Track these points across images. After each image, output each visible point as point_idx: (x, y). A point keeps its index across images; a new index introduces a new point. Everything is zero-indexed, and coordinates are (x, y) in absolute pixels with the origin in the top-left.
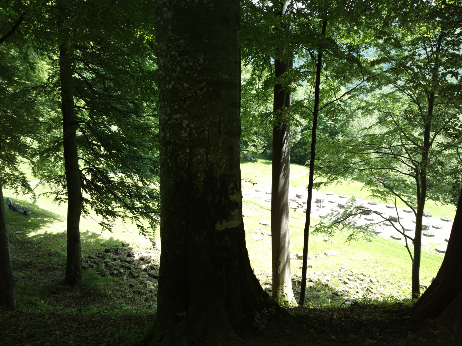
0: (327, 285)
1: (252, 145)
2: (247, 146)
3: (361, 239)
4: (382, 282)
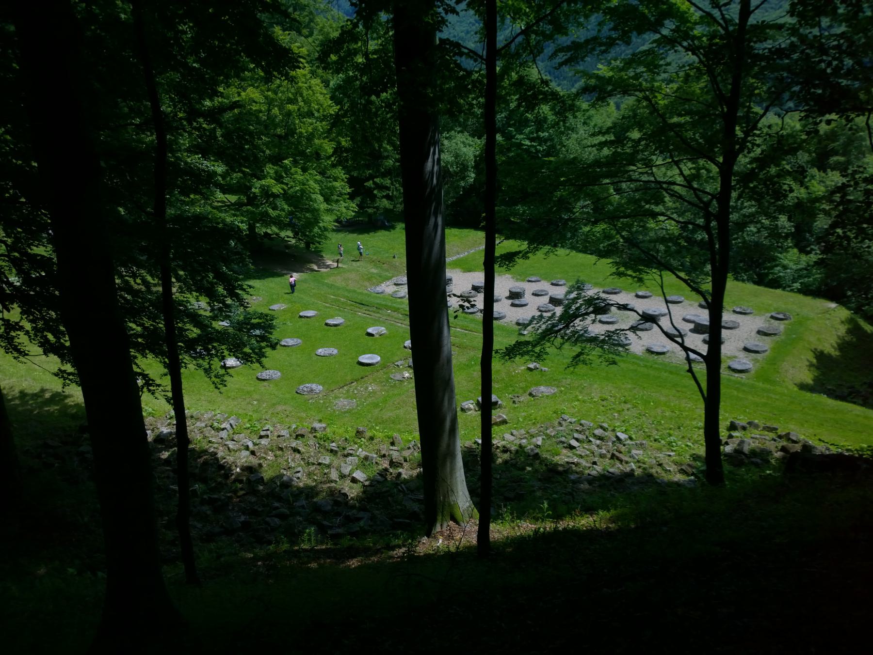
0: (537, 454)
1: (384, 197)
2: (373, 198)
4: (639, 439)
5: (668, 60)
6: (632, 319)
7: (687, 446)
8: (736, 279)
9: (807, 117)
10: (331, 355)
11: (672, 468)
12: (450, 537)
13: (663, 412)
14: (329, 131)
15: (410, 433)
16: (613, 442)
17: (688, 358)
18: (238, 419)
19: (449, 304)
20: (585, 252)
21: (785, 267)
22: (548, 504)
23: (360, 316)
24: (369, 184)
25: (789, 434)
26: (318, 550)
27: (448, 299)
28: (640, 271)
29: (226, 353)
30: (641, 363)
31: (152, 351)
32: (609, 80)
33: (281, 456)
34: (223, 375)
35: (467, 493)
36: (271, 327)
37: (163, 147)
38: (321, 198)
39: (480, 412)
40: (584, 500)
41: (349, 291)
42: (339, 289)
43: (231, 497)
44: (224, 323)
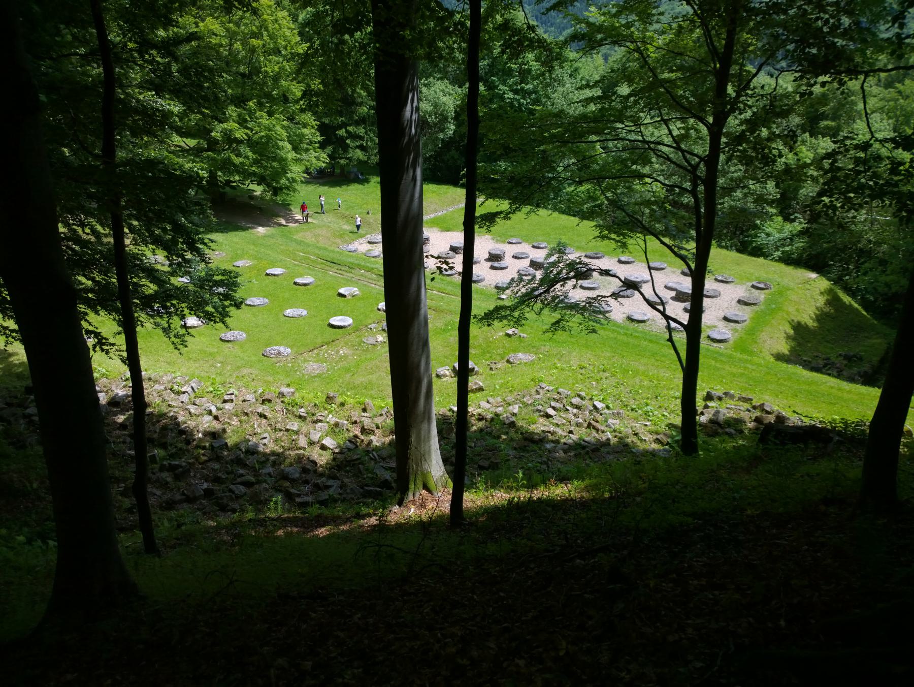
0: (513, 423)
1: (357, 147)
2: (346, 148)
3: (576, 329)
4: (616, 407)
5: (661, 9)
6: (614, 285)
7: (664, 415)
8: (720, 246)
9: (801, 77)
10: (300, 316)
11: (648, 437)
12: (423, 505)
13: (641, 381)
14: (298, 72)
15: (383, 399)
16: (591, 411)
17: (668, 327)
18: (200, 382)
19: (426, 265)
20: (570, 215)
21: (768, 235)
22: (523, 474)
23: (331, 276)
24: (342, 132)
25: (763, 404)
26: (284, 520)
27: (425, 260)
28: (624, 235)
29: (186, 311)
30: (622, 331)
31: (105, 308)
32: (600, 28)
33: (247, 422)
34: (184, 335)
35: (441, 462)
36: (236, 284)
37: (110, 81)
38: (290, 147)
39: (456, 379)
40: (559, 469)
41: (320, 248)
42: (309, 245)
43: (193, 464)
44: (185, 280)
